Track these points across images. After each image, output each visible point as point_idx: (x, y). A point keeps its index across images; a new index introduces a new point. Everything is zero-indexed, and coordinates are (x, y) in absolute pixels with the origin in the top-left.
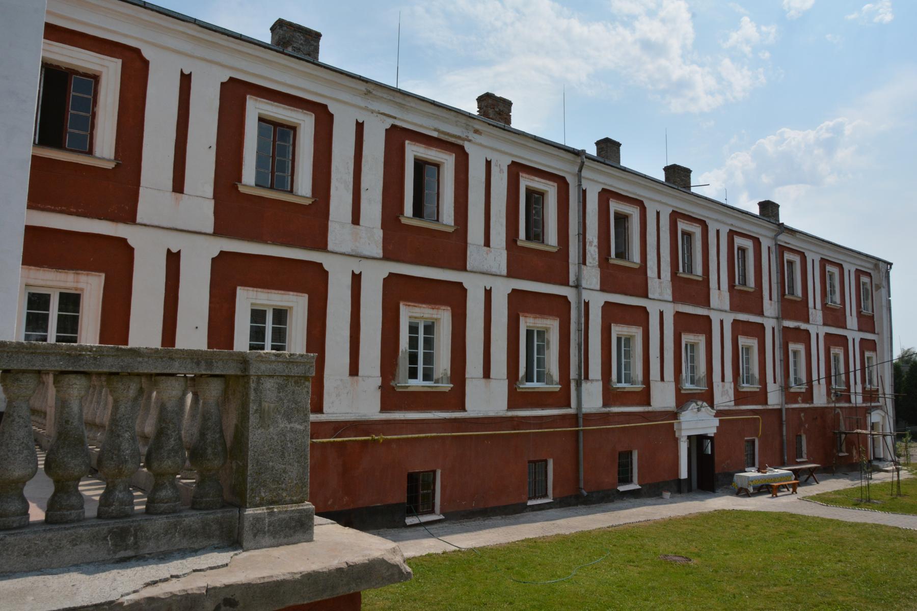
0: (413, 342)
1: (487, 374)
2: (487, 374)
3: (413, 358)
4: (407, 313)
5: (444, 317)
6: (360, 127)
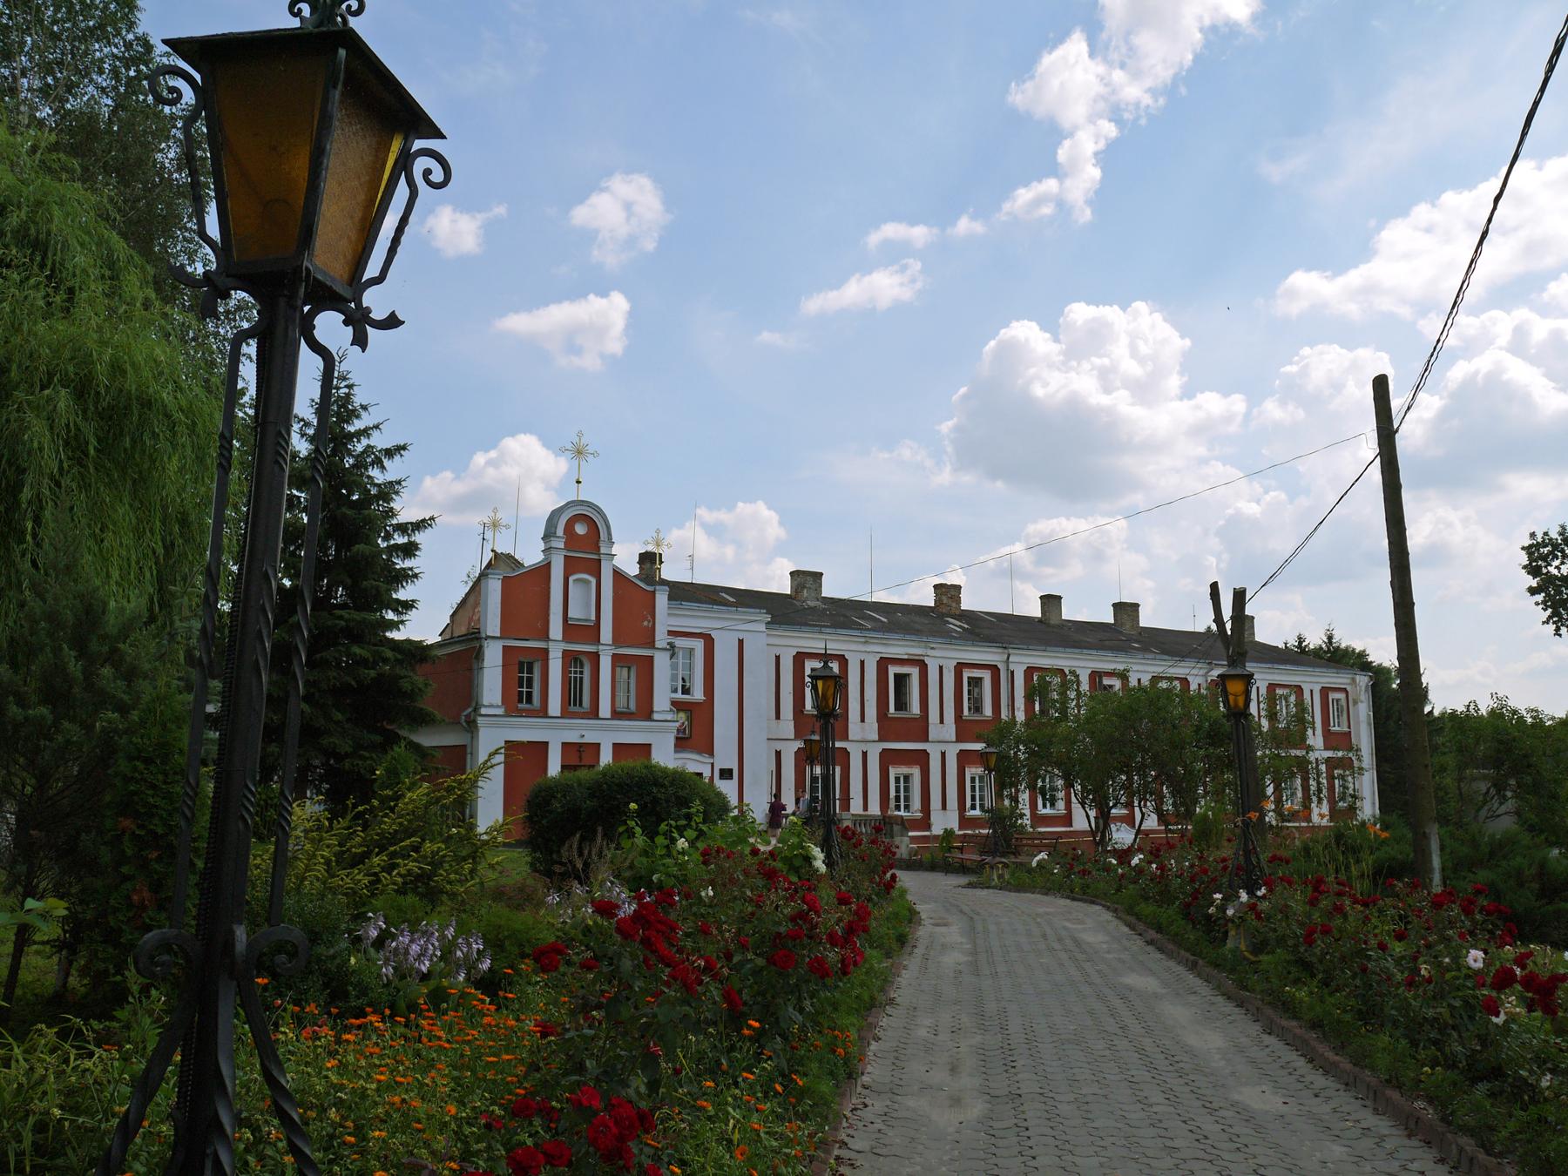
0: (898, 790)
1: (944, 807)
2: (944, 807)
3: (897, 798)
4: (893, 772)
5: (916, 772)
6: (862, 663)
